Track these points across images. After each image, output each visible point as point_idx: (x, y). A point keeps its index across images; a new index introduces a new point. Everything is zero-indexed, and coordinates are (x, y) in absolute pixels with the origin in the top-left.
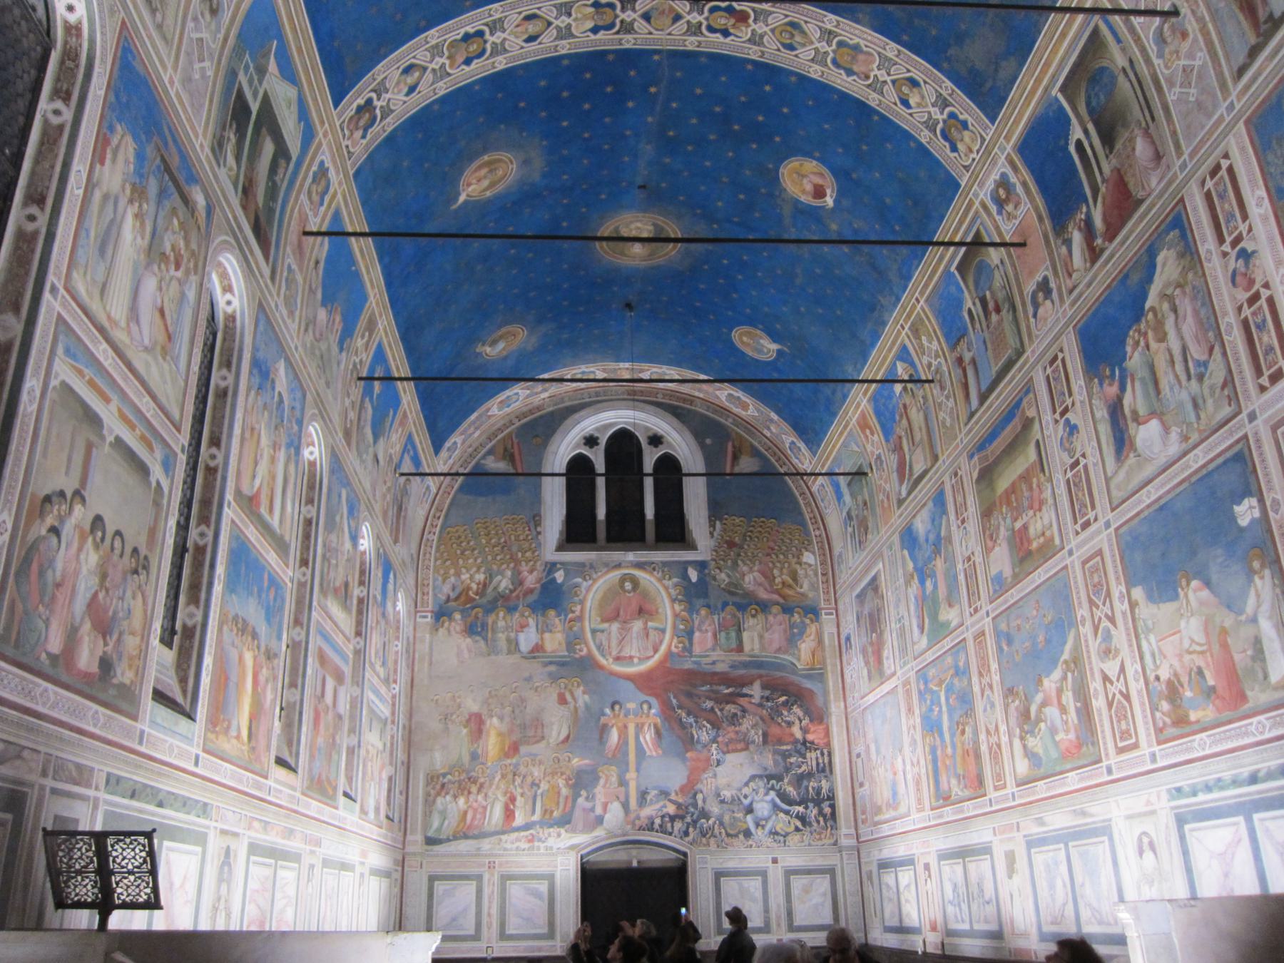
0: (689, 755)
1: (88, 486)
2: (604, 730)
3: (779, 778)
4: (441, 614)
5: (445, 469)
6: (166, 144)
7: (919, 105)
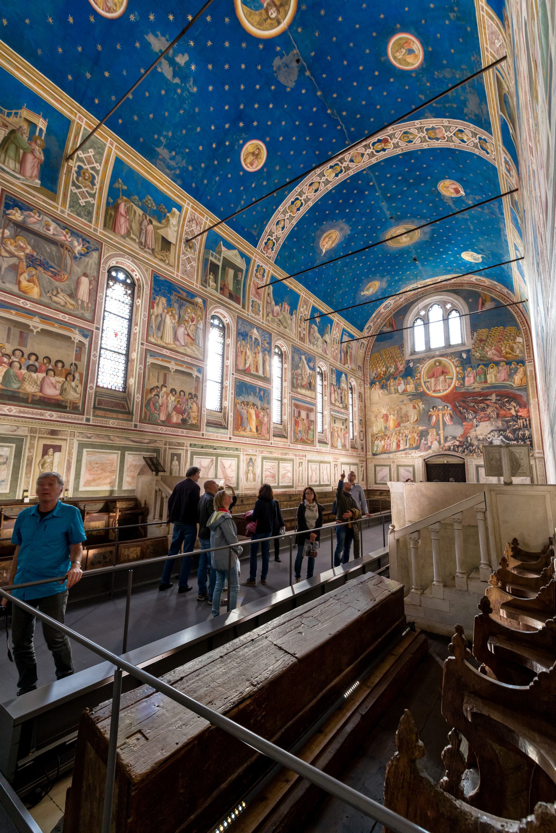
0: (464, 424)
1: (167, 383)
2: (430, 417)
3: (505, 431)
4: (372, 383)
5: (369, 335)
6: (179, 293)
7: (468, 139)
